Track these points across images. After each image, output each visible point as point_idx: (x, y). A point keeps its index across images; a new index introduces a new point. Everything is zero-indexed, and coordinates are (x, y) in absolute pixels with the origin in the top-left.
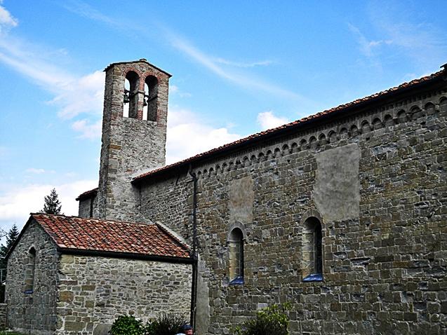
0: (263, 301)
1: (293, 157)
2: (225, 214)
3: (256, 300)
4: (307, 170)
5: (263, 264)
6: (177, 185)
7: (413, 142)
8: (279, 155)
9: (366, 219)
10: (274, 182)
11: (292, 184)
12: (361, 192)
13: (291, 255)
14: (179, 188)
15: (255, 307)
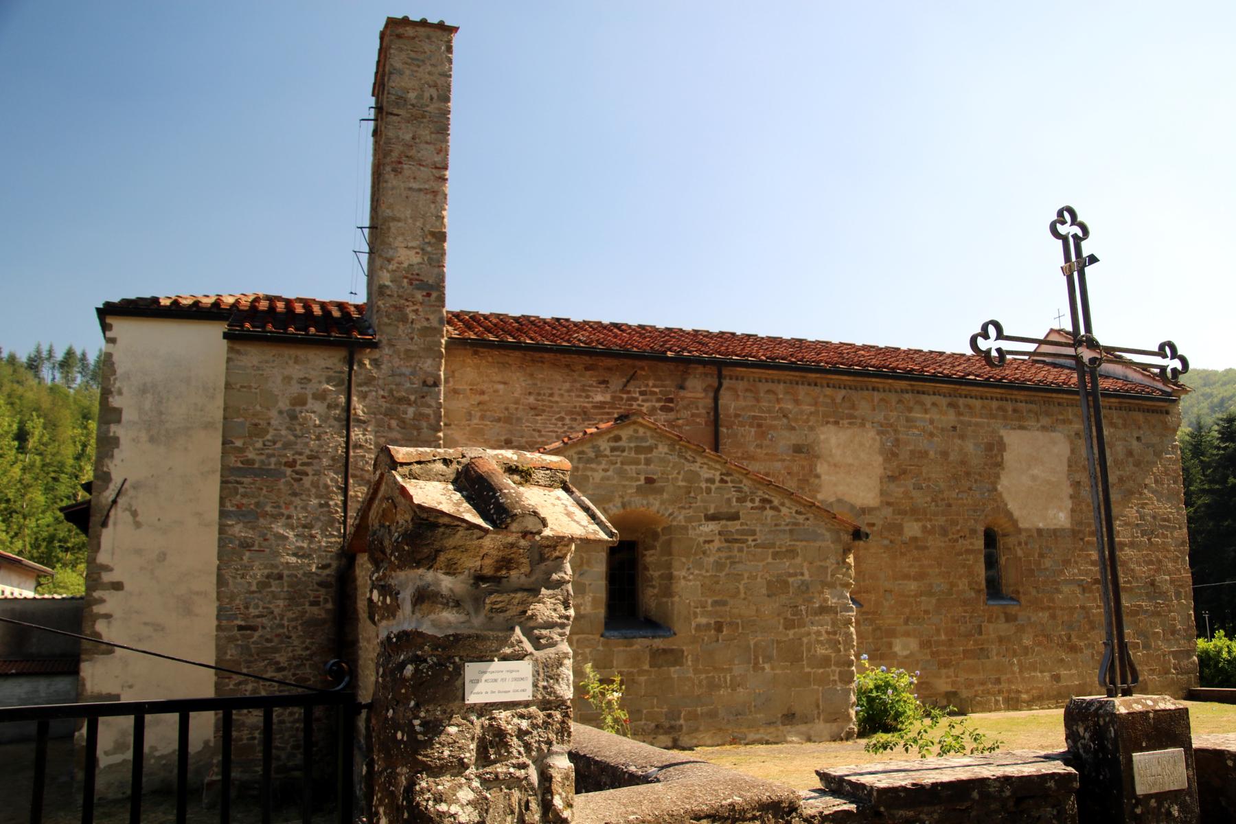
0: (907, 634)
1: (962, 422)
2: (809, 477)
3: (891, 633)
4: (989, 447)
5: (906, 577)
6: (623, 390)
7: (1130, 453)
8: (934, 414)
9: (1079, 531)
10: (926, 453)
11: (963, 463)
12: (1071, 497)
13: (964, 567)
14: (636, 399)
15: (890, 645)
